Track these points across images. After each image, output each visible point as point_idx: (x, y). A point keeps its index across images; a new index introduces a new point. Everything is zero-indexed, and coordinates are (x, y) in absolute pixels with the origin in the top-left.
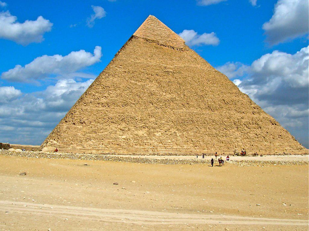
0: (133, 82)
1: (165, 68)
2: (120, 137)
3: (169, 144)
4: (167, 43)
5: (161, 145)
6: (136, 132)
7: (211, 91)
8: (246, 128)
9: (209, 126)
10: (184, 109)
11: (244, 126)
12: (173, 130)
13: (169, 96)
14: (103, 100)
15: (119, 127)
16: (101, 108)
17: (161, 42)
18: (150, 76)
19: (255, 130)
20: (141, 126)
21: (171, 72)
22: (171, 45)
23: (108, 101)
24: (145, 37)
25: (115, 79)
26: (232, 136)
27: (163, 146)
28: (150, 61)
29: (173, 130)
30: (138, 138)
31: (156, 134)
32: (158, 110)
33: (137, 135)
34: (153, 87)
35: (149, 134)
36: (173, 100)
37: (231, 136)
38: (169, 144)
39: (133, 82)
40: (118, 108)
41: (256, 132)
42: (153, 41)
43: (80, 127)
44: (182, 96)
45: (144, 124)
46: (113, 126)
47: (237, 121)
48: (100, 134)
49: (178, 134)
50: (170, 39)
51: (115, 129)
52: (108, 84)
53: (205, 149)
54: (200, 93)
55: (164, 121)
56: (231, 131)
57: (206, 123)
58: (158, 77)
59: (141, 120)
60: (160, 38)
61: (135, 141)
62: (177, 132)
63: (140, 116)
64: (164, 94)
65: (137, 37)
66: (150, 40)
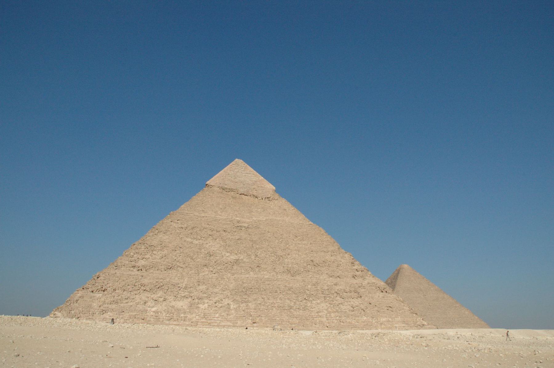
0: (189, 240)
1: (238, 222)
2: (149, 309)
3: (216, 319)
6: (173, 303)
8: (338, 298)
10: (251, 273)
11: (335, 294)
12: (226, 301)
13: (233, 257)
14: (142, 263)
15: (152, 296)
16: (135, 272)
17: (241, 191)
18: (215, 232)
20: (183, 295)
21: (245, 227)
24: (221, 185)
26: (314, 309)
27: (205, 322)
28: (220, 214)
29: (226, 301)
30: (173, 311)
31: (200, 306)
32: (214, 275)
33: (173, 307)
34: (213, 246)
35: (191, 305)
36: (237, 262)
37: (312, 309)
39: (189, 240)
40: (157, 272)
42: (231, 190)
46: (144, 296)
48: (122, 305)
49: (232, 307)
51: (147, 299)
52: (155, 242)
55: (217, 290)
56: (314, 302)
57: (278, 291)
58: (224, 234)
59: (186, 288)
61: (168, 315)
62: (232, 303)
63: (186, 283)
64: (228, 254)
66: (227, 188)
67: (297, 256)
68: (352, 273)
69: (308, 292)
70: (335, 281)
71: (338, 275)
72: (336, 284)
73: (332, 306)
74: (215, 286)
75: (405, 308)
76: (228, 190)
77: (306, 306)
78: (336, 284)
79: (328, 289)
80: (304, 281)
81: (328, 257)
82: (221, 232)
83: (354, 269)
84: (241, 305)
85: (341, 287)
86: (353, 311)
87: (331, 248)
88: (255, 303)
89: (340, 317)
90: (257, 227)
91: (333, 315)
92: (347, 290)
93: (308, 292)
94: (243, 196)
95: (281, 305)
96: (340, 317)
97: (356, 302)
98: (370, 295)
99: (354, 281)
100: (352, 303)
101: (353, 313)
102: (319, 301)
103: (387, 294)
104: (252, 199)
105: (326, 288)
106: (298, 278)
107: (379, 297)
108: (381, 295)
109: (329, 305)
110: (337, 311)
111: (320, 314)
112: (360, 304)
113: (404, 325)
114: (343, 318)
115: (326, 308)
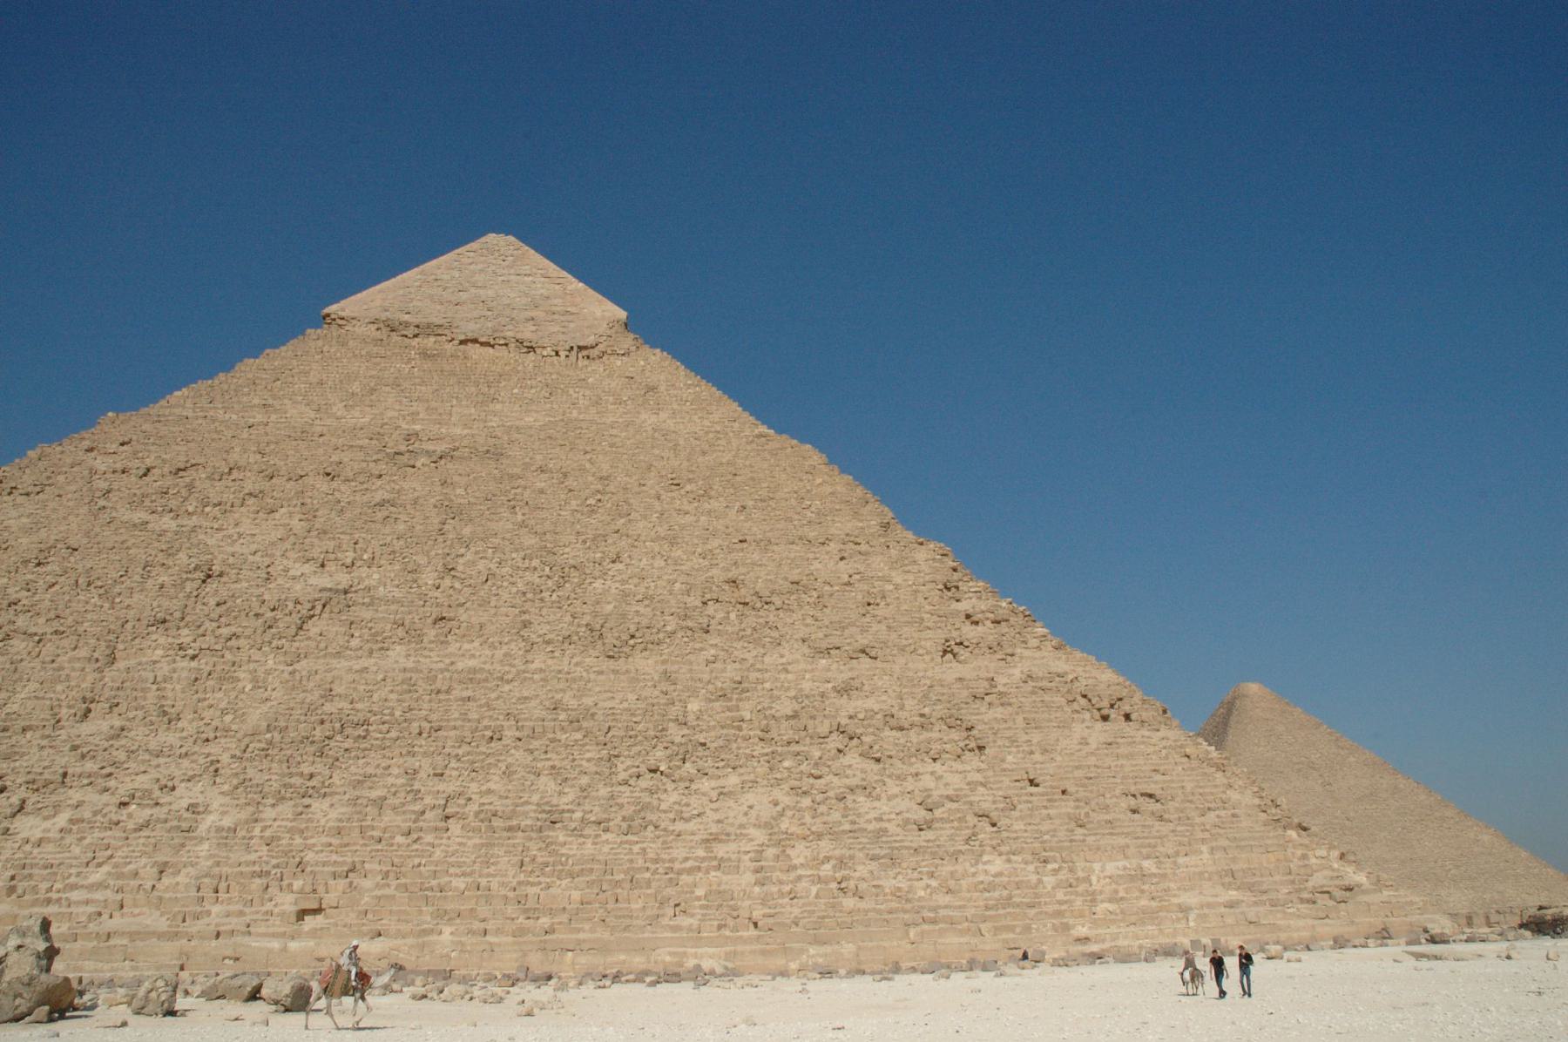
8: (852, 759)
11: (835, 741)
17: (470, 329)
24: (383, 316)
26: (691, 826)
54: (572, 553)
56: (705, 785)
57: (510, 734)
66: (407, 325)
67: (659, 562)
68: (941, 635)
69: (676, 733)
70: (840, 671)
71: (863, 641)
72: (845, 690)
73: (806, 802)
74: (170, 719)
75: (1234, 796)
76: (410, 332)
77: (646, 807)
78: (845, 690)
79: (795, 716)
80: (667, 676)
81: (825, 565)
82: (309, 480)
83: (955, 614)
84: (269, 813)
85: (870, 703)
86: (929, 825)
87: (841, 525)
88: (354, 802)
89: (841, 863)
90: (496, 454)
91: (799, 853)
92: (907, 715)
93: (676, 733)
94: (474, 351)
95: (498, 805)
96: (841, 863)
97: (948, 777)
98: (1036, 737)
99: (951, 671)
100: (928, 781)
101: (929, 835)
102: (733, 780)
103: (1129, 729)
104: (512, 355)
105: (785, 707)
106: (645, 664)
107: (1084, 742)
108: (1099, 733)
109: (786, 800)
110: (833, 834)
111: (721, 850)
112: (973, 785)
113: (1233, 894)
114: (862, 871)
115: (767, 812)
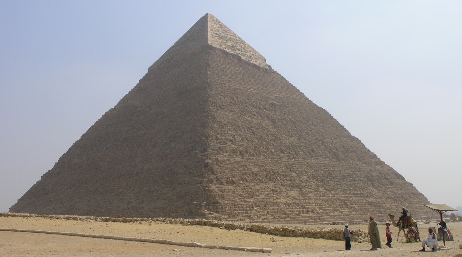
4: (250, 59)
5: (321, 211)
7: (326, 134)
9: (349, 183)
13: (293, 140)
19: (388, 186)
22: (256, 63)
23: (239, 148)
25: (227, 113)
38: (329, 210)
41: (391, 189)
42: (233, 55)
43: (231, 187)
44: (303, 140)
45: (289, 182)
47: (369, 175)
50: (250, 54)
53: (362, 214)
58: (268, 112)
60: (238, 52)
65: (214, 47)
